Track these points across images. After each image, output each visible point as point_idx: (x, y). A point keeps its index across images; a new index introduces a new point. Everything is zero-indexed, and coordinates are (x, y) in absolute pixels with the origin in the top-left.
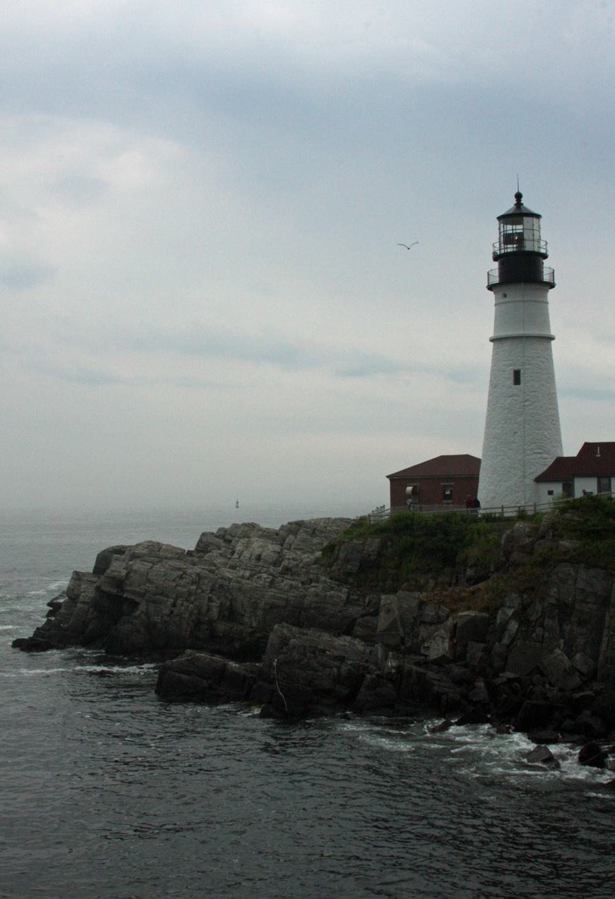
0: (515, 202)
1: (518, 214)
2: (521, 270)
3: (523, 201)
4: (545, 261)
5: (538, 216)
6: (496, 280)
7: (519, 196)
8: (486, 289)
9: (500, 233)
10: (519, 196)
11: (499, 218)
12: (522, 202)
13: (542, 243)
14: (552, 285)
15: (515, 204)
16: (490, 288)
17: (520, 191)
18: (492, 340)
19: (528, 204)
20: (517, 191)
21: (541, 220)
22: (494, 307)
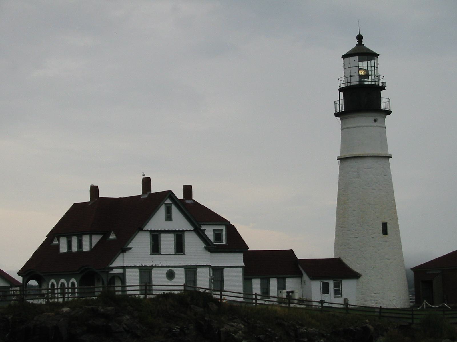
0: (357, 43)
1: (362, 53)
2: (362, 100)
5: (377, 55)
6: (342, 109)
7: (360, 38)
10: (360, 38)
11: (344, 57)
12: (363, 43)
13: (381, 77)
14: (389, 112)
15: (357, 45)
16: (337, 115)
17: (360, 34)
18: (342, 159)
20: (359, 34)
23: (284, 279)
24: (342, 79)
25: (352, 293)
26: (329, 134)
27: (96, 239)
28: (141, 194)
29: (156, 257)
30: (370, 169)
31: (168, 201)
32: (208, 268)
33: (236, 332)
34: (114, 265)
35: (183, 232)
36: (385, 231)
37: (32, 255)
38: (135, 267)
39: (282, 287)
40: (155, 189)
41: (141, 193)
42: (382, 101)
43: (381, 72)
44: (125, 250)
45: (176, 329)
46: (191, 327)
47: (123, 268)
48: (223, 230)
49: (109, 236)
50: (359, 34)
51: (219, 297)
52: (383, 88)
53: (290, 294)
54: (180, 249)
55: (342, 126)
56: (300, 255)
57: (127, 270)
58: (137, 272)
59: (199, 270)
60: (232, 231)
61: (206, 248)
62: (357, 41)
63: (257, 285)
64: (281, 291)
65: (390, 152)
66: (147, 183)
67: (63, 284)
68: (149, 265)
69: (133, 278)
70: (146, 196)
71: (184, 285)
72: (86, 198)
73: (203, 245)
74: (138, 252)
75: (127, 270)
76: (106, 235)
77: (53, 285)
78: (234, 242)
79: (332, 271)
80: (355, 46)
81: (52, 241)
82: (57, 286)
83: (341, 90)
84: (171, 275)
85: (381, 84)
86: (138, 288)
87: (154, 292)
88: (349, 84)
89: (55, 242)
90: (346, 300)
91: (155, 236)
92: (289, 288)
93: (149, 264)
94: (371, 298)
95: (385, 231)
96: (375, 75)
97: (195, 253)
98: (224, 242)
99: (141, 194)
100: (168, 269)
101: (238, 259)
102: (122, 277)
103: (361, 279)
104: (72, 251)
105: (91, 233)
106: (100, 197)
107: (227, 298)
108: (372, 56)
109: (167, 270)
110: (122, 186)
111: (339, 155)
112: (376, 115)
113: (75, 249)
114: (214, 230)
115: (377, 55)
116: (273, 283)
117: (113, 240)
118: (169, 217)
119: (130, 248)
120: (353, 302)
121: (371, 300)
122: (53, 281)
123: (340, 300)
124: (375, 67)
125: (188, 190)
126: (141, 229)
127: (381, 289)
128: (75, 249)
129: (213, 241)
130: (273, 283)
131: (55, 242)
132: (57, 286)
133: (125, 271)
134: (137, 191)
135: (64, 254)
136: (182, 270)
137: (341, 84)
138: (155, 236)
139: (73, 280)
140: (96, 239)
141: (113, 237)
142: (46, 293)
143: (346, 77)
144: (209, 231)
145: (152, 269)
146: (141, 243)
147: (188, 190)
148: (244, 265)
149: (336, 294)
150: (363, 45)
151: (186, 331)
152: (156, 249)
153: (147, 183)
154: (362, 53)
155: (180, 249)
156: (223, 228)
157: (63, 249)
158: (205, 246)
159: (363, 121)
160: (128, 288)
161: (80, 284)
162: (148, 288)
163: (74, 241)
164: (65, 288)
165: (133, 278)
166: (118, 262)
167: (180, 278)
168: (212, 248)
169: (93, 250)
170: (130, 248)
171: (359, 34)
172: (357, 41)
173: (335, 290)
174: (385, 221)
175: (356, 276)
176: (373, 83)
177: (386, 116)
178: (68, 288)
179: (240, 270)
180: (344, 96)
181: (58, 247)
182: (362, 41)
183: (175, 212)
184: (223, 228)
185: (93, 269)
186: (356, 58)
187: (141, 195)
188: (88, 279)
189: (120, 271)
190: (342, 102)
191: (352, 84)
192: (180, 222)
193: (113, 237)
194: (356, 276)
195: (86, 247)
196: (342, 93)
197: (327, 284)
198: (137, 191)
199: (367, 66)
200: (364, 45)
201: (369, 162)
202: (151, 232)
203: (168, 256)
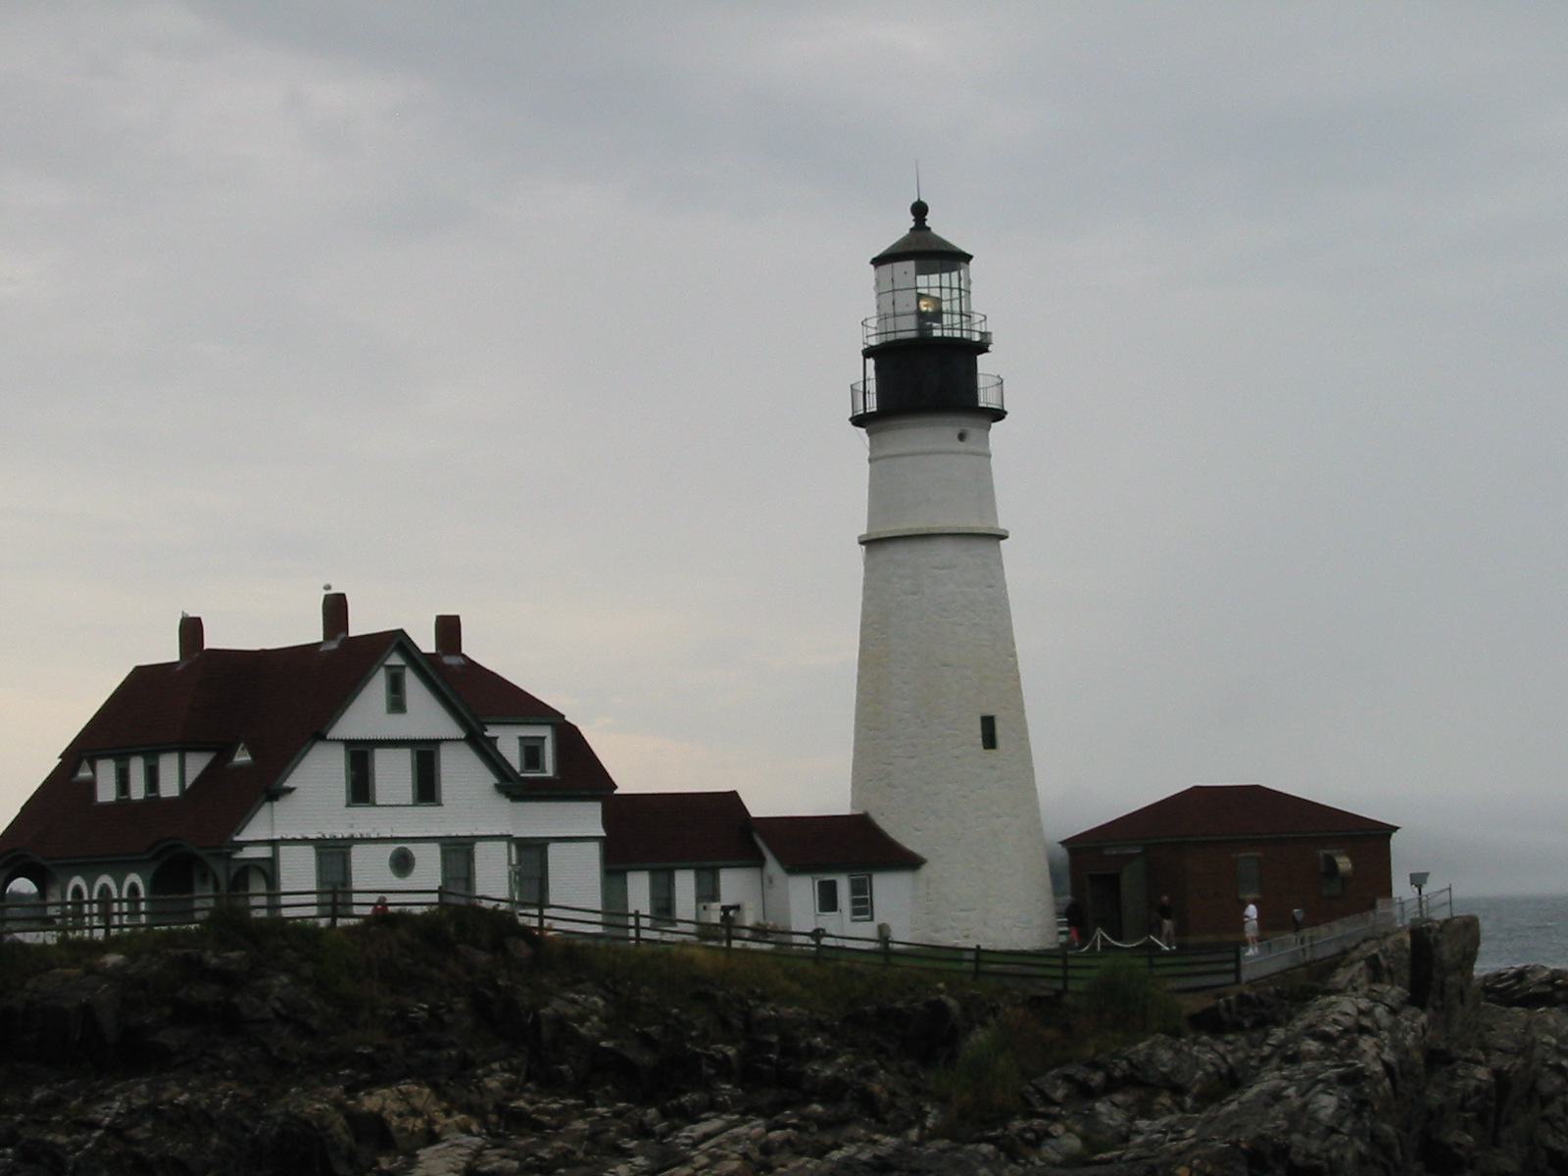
0: (913, 224)
2: (926, 380)
4: (980, 358)
5: (967, 258)
6: (872, 406)
7: (920, 210)
8: (850, 423)
10: (920, 210)
11: (878, 262)
12: (927, 224)
13: (977, 318)
14: (998, 415)
15: (911, 230)
16: (858, 421)
17: (922, 199)
18: (870, 543)
19: (938, 224)
20: (916, 200)
22: (868, 465)
23: (714, 872)
24: (873, 323)
25: (901, 910)
26: (835, 474)
27: (197, 764)
28: (321, 639)
29: (361, 812)
31: (395, 660)
32: (504, 844)
33: (582, 1019)
34: (246, 835)
35: (437, 742)
36: (989, 741)
37: (19, 811)
38: (305, 841)
39: (708, 893)
40: (361, 623)
41: (320, 638)
42: (982, 382)
43: (977, 304)
44: (275, 793)
45: (419, 1010)
46: (460, 1004)
47: (273, 843)
48: (543, 738)
49: (234, 755)
51: (535, 923)
52: (982, 347)
53: (731, 913)
54: (427, 790)
55: (872, 450)
56: (758, 807)
57: (283, 849)
58: (309, 852)
59: (480, 848)
60: (570, 740)
61: (499, 788)
63: (639, 890)
64: (704, 904)
65: (1003, 524)
66: (336, 609)
67: (105, 889)
68: (339, 835)
69: (299, 873)
70: (333, 646)
71: (440, 891)
72: (168, 651)
73: (493, 780)
74: (312, 799)
75: (283, 849)
76: (224, 752)
77: (77, 891)
78: (578, 771)
79: (845, 848)
80: (907, 232)
81: (76, 770)
82: (90, 896)
83: (868, 353)
84: (402, 863)
85: (977, 338)
86: (313, 899)
87: (356, 910)
88: (891, 337)
89: (85, 774)
90: (883, 930)
91: (360, 755)
92: (727, 897)
93: (342, 832)
94: (953, 924)
95: (989, 741)
96: (961, 311)
97: (470, 799)
98: (549, 770)
99: (321, 639)
100: (392, 847)
101: (587, 818)
102: (269, 870)
103: (925, 870)
104: (129, 799)
105: (183, 748)
106: (208, 650)
107: (558, 925)
108: (951, 259)
109: (392, 847)
110: (265, 615)
111: (863, 530)
112: (965, 423)
113: (138, 791)
114: (521, 738)
115: (967, 258)
116: (685, 884)
117: (241, 767)
118: (397, 704)
119: (290, 790)
120: (903, 934)
121: (952, 928)
122: (78, 881)
123: (868, 929)
124: (960, 289)
125: (449, 629)
126: (321, 737)
127: (977, 899)
128: (138, 791)
129: (518, 770)
130: (685, 884)
131: (85, 774)
132: (90, 896)
133: (276, 853)
134: (310, 631)
135: (107, 806)
136: (435, 850)
137: (867, 337)
138: (360, 755)
139: (134, 878)
140: (197, 764)
141: (242, 757)
142: (59, 913)
143: (882, 317)
144: (509, 742)
145: (350, 847)
146: (319, 774)
147: (449, 629)
148: (604, 834)
149: (855, 912)
150: (929, 229)
151: (447, 1018)
152: (361, 791)
153: (336, 609)
154: (925, 251)
155: (427, 790)
156: (546, 732)
157: (106, 792)
158: (496, 781)
159: (927, 440)
160: (284, 900)
161: (154, 887)
162: (340, 899)
163: (137, 768)
164: (112, 900)
165: (299, 873)
166: (260, 828)
167: (429, 870)
168: (515, 788)
169: (190, 794)
170: (290, 790)
173: (855, 902)
174: (988, 712)
175: (909, 862)
176: (957, 334)
177: (993, 425)
178: (120, 901)
179: (594, 850)
180: (878, 369)
181: (90, 786)
183: (415, 689)
184: (546, 732)
185: (187, 849)
186: (910, 266)
187: (318, 644)
188: (175, 873)
189: (264, 852)
190: (872, 386)
192: (425, 716)
193: (242, 757)
194: (909, 862)
195: (169, 788)
196: (871, 362)
197: (833, 884)
198: (310, 631)
199: (941, 287)
200: (933, 230)
201: (946, 551)
202: (349, 744)
203: (396, 811)
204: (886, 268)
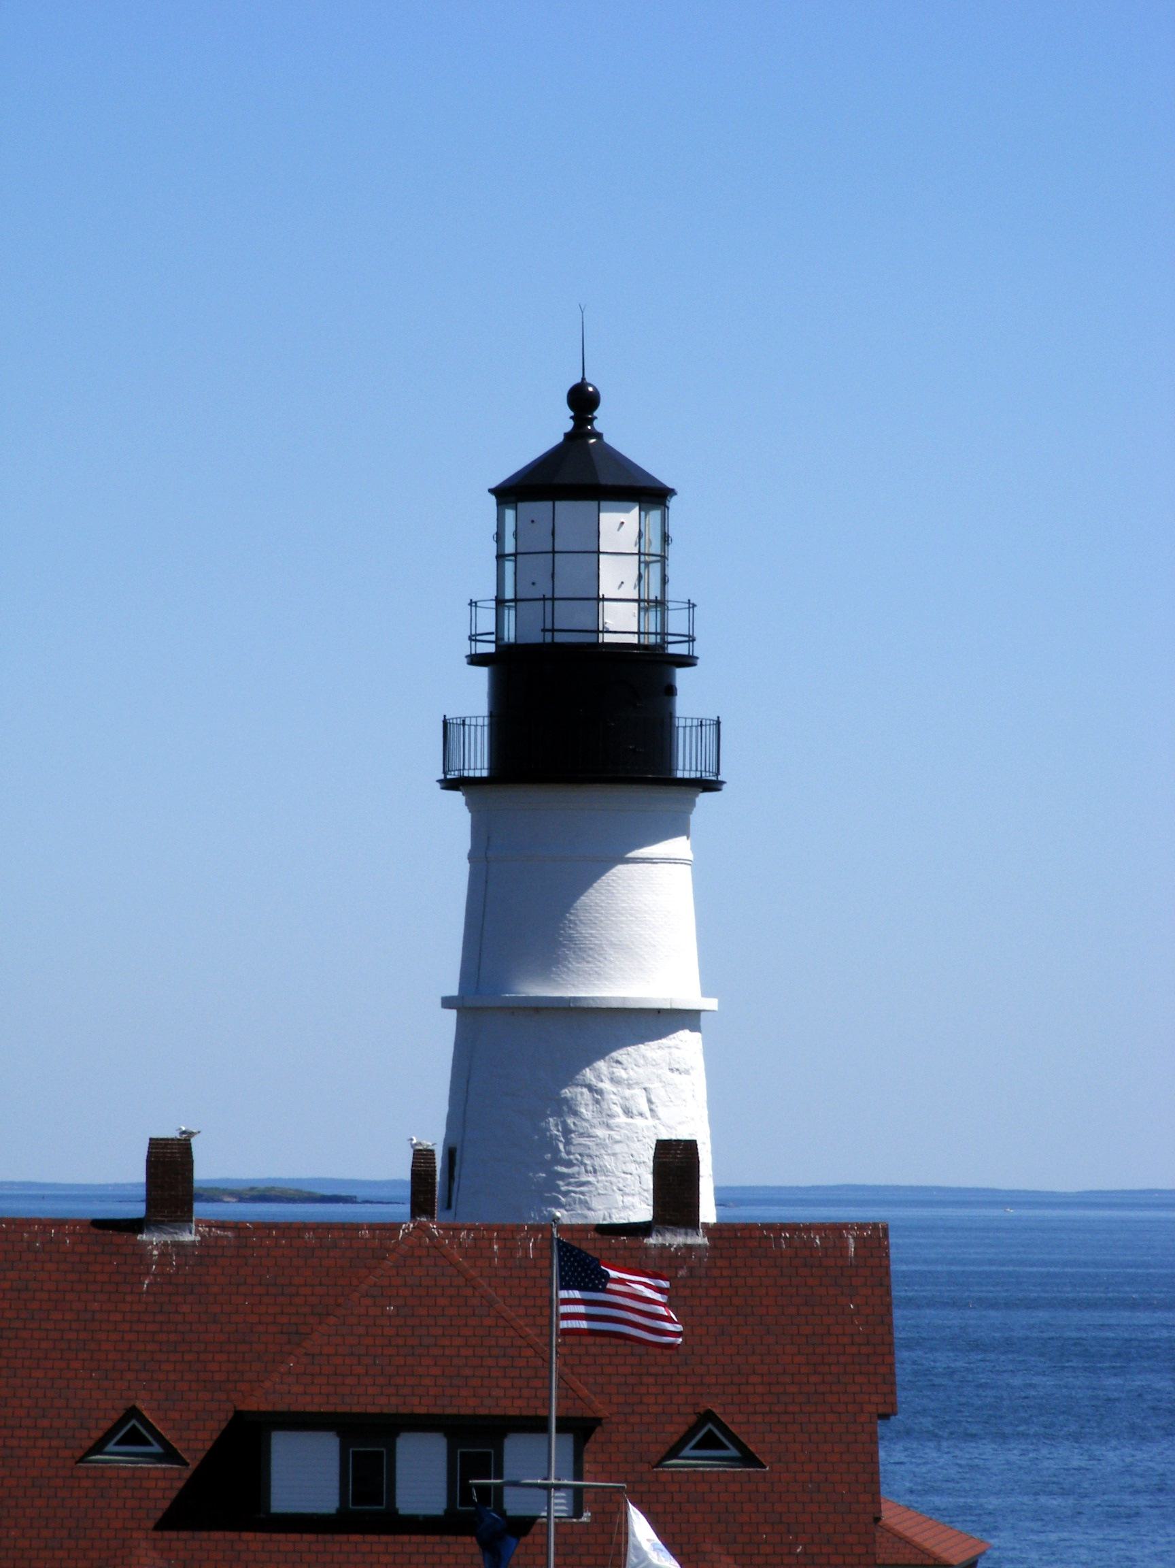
0: (569, 425)
1: (576, 474)
3: (603, 420)
7: (583, 401)
9: (501, 557)
10: (583, 401)
15: (568, 436)
20: (579, 380)
21: (673, 503)
30: (687, 1072)
50: (583, 379)
62: (572, 414)
80: (559, 439)
137: (544, 630)
171: (583, 379)
172: (572, 414)
182: (595, 414)
191: (608, 638)
200: (607, 439)
204: (567, 510)
